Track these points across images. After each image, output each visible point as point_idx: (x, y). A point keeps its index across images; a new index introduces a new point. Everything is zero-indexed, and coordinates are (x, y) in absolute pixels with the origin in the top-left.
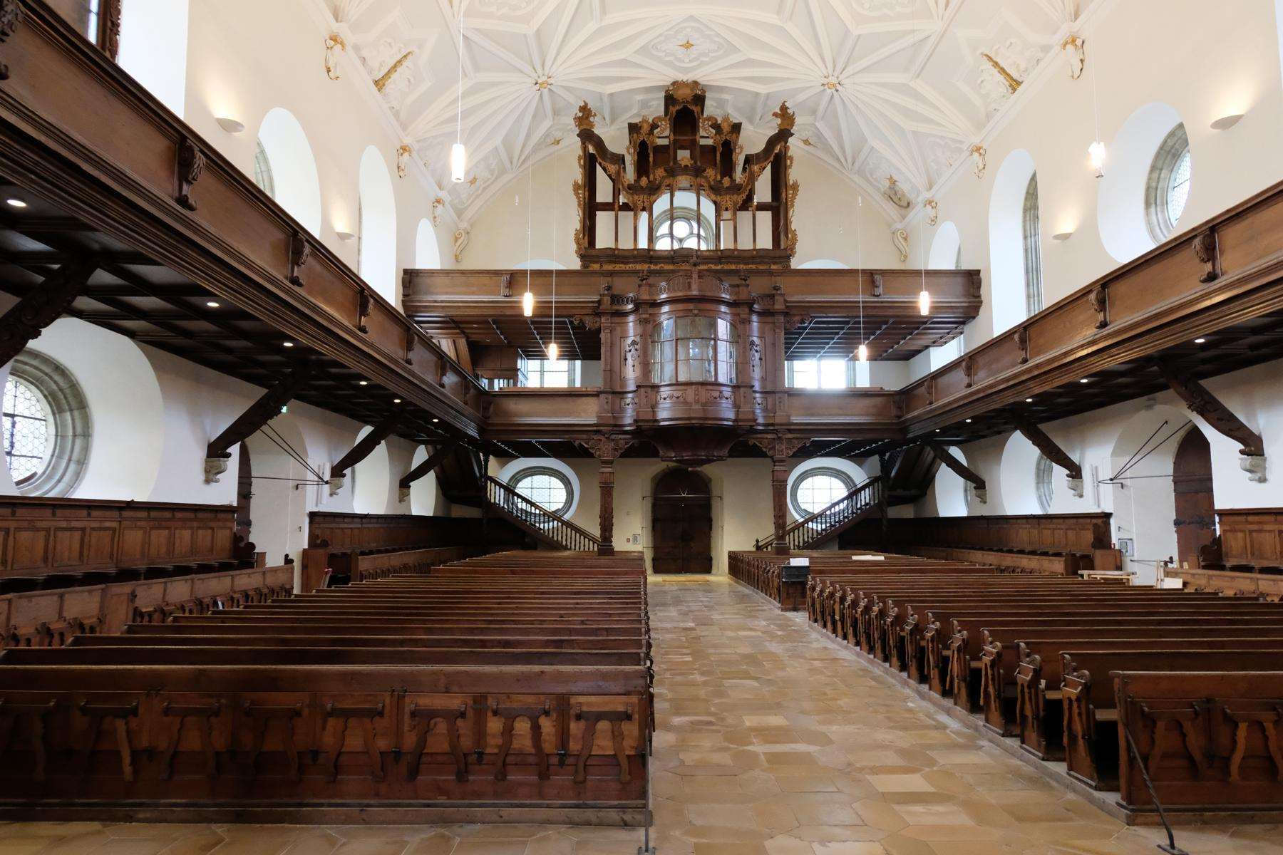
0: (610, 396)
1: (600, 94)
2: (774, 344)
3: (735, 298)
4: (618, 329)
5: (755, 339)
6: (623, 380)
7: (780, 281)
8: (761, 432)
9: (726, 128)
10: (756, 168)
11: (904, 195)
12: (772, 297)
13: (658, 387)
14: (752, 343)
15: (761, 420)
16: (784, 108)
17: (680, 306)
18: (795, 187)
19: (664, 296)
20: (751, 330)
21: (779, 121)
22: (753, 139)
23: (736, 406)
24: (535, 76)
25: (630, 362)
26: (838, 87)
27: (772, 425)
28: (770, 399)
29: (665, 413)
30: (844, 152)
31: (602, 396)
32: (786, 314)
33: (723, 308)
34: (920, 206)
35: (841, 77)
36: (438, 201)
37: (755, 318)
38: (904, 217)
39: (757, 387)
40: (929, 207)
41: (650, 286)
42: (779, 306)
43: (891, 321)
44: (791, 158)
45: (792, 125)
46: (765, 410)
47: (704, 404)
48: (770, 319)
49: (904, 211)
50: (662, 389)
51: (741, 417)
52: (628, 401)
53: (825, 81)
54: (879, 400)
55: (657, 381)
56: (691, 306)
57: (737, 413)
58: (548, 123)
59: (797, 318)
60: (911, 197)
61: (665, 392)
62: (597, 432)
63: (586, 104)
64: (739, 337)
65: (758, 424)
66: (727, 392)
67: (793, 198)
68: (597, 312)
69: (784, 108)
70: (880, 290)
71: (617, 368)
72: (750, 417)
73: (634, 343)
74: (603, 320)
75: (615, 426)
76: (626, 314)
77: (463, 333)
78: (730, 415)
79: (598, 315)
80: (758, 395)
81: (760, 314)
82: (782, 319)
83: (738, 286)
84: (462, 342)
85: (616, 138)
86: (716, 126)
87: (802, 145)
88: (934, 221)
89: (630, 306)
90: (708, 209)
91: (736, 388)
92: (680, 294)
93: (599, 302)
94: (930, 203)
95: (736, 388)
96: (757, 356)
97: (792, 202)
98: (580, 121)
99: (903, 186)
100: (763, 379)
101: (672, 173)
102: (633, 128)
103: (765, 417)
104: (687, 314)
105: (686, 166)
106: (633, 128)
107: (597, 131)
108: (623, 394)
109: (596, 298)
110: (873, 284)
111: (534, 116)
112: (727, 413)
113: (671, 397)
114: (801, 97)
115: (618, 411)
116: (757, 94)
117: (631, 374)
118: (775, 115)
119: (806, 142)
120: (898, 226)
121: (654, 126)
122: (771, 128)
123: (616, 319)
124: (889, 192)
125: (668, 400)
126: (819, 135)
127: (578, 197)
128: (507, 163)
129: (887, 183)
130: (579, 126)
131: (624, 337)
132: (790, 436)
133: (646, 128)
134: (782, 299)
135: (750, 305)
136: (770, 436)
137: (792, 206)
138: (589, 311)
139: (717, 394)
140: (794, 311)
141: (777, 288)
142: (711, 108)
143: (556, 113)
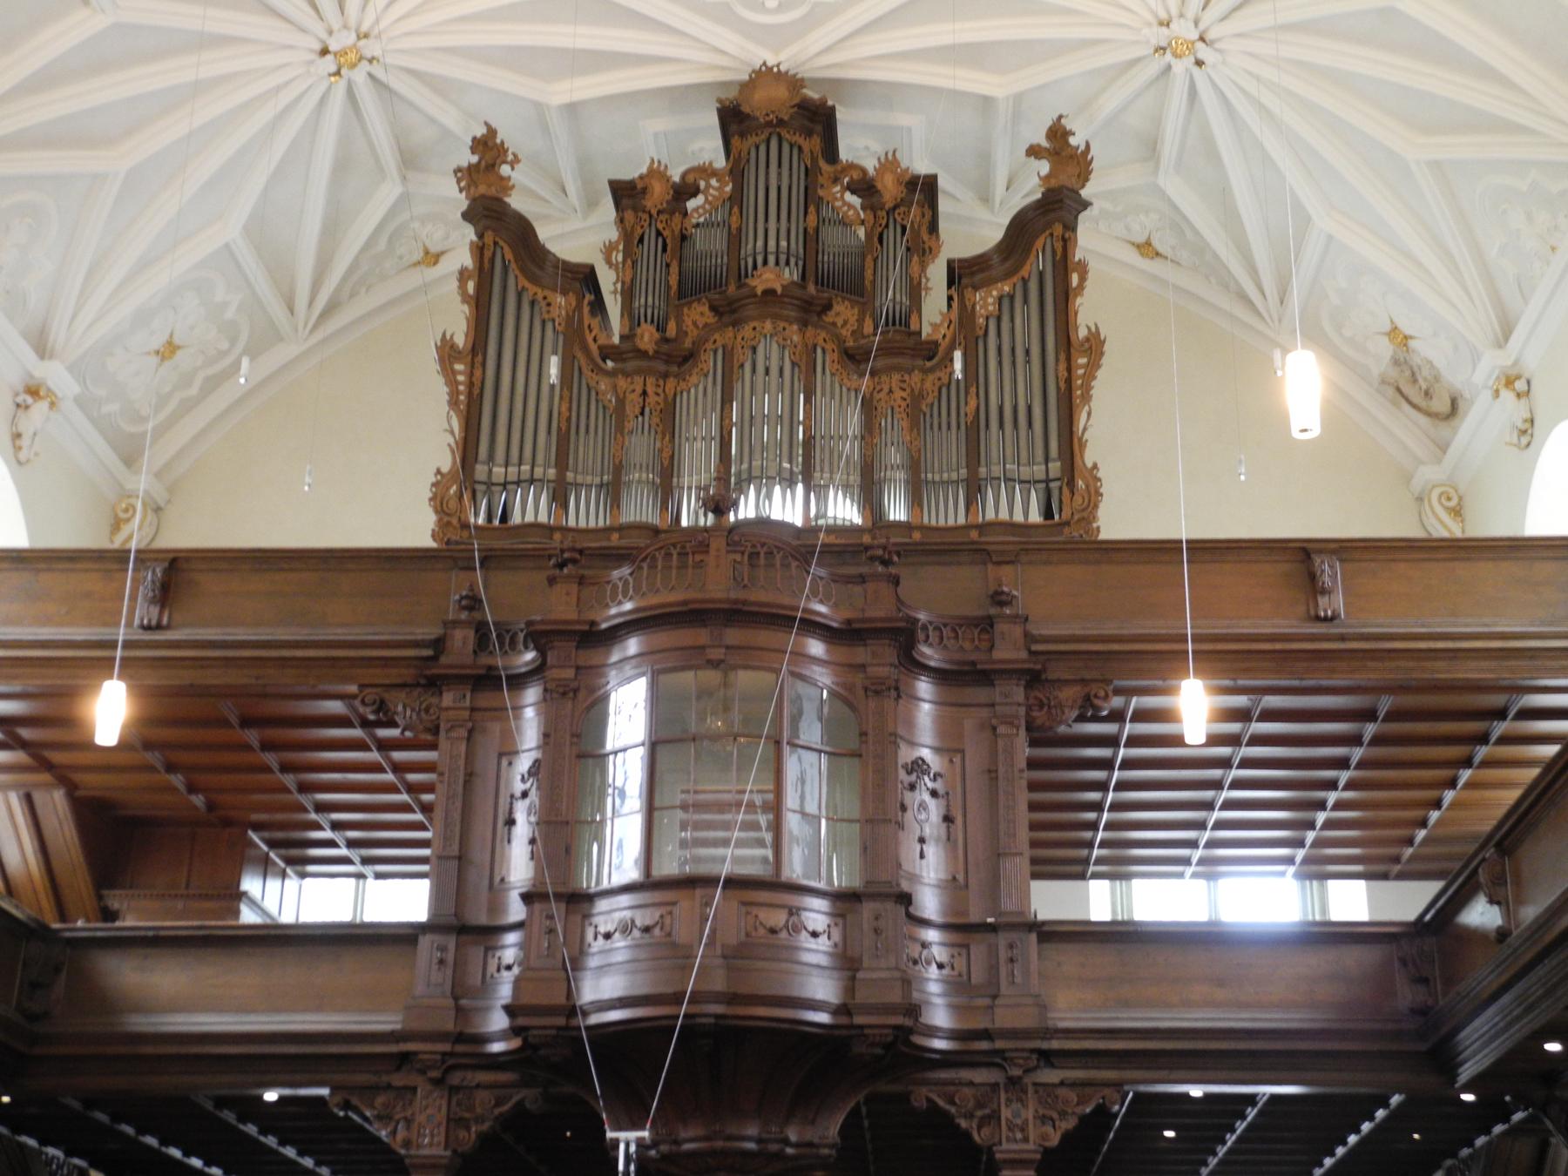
0: (451, 942)
1: (538, 105)
2: (992, 773)
3: (848, 614)
4: (495, 728)
5: (926, 753)
6: (496, 888)
7: (1007, 578)
8: (947, 1060)
9: (890, 189)
10: (985, 302)
11: (1437, 378)
12: (986, 624)
13: (589, 898)
14: (918, 766)
15: (940, 1016)
16: (1058, 133)
17: (665, 638)
18: (1095, 346)
19: (628, 606)
20: (910, 723)
21: (1044, 167)
22: (973, 224)
23: (847, 963)
24: (319, 29)
25: (523, 829)
26: (1203, 52)
27: (985, 1034)
28: (978, 951)
29: (607, 983)
30: (1253, 272)
31: (425, 941)
32: (1033, 679)
33: (816, 648)
34: (1487, 395)
35: (1208, 17)
36: (34, 392)
37: (924, 687)
38: (1443, 448)
39: (929, 903)
40: (1507, 396)
41: (581, 581)
42: (1008, 651)
43: (1385, 704)
44: (1083, 269)
45: (1084, 174)
46: (959, 987)
47: (738, 955)
48: (981, 694)
49: (1443, 430)
50: (602, 905)
51: (862, 996)
52: (509, 955)
53: (1161, 36)
54: (1355, 958)
55: (588, 883)
56: (700, 636)
57: (850, 987)
58: (389, 192)
59: (1068, 694)
60: (1456, 376)
61: (610, 914)
62: (404, 1059)
63: (492, 132)
64: (866, 747)
65: (932, 1031)
66: (816, 914)
67: (1090, 376)
68: (430, 673)
69: (1058, 133)
70: (1336, 602)
71: (479, 855)
72: (895, 997)
73: (535, 770)
74: (448, 699)
75: (460, 1038)
76: (518, 682)
77: (48, 766)
78: (822, 988)
79: (434, 684)
80: (932, 935)
81: (942, 677)
82: (1019, 694)
83: (862, 579)
84: (55, 804)
85: (578, 231)
86: (865, 187)
87: (1133, 257)
88: (1527, 433)
89: (530, 656)
90: (843, 421)
91: (845, 901)
92: (672, 597)
93: (439, 644)
94: (1509, 382)
95: (845, 901)
96: (934, 809)
97: (1087, 389)
98: (468, 176)
99: (1430, 350)
100: (954, 887)
101: (728, 312)
102: (625, 194)
103: (956, 1009)
104: (694, 658)
105: (770, 292)
106: (625, 194)
107: (516, 202)
108: (490, 933)
109: (430, 632)
110: (1313, 586)
111: (342, 166)
112: (816, 983)
113: (626, 928)
114: (1110, 103)
115: (465, 995)
116: (987, 102)
117: (519, 866)
118: (1034, 152)
119: (1146, 248)
120: (1428, 474)
121: (685, 190)
122: (1029, 183)
123: (486, 699)
124: (1393, 373)
125: (619, 942)
126: (1179, 223)
127: (451, 382)
128: (278, 311)
129: (1385, 349)
130: (467, 189)
131: (509, 752)
132: (1050, 1076)
133: (658, 195)
134: (1018, 631)
135: (903, 637)
136: (981, 1076)
137: (1086, 397)
138: (407, 674)
139: (778, 918)
140: (1056, 672)
141: (999, 599)
142: (858, 144)
143: (409, 161)
